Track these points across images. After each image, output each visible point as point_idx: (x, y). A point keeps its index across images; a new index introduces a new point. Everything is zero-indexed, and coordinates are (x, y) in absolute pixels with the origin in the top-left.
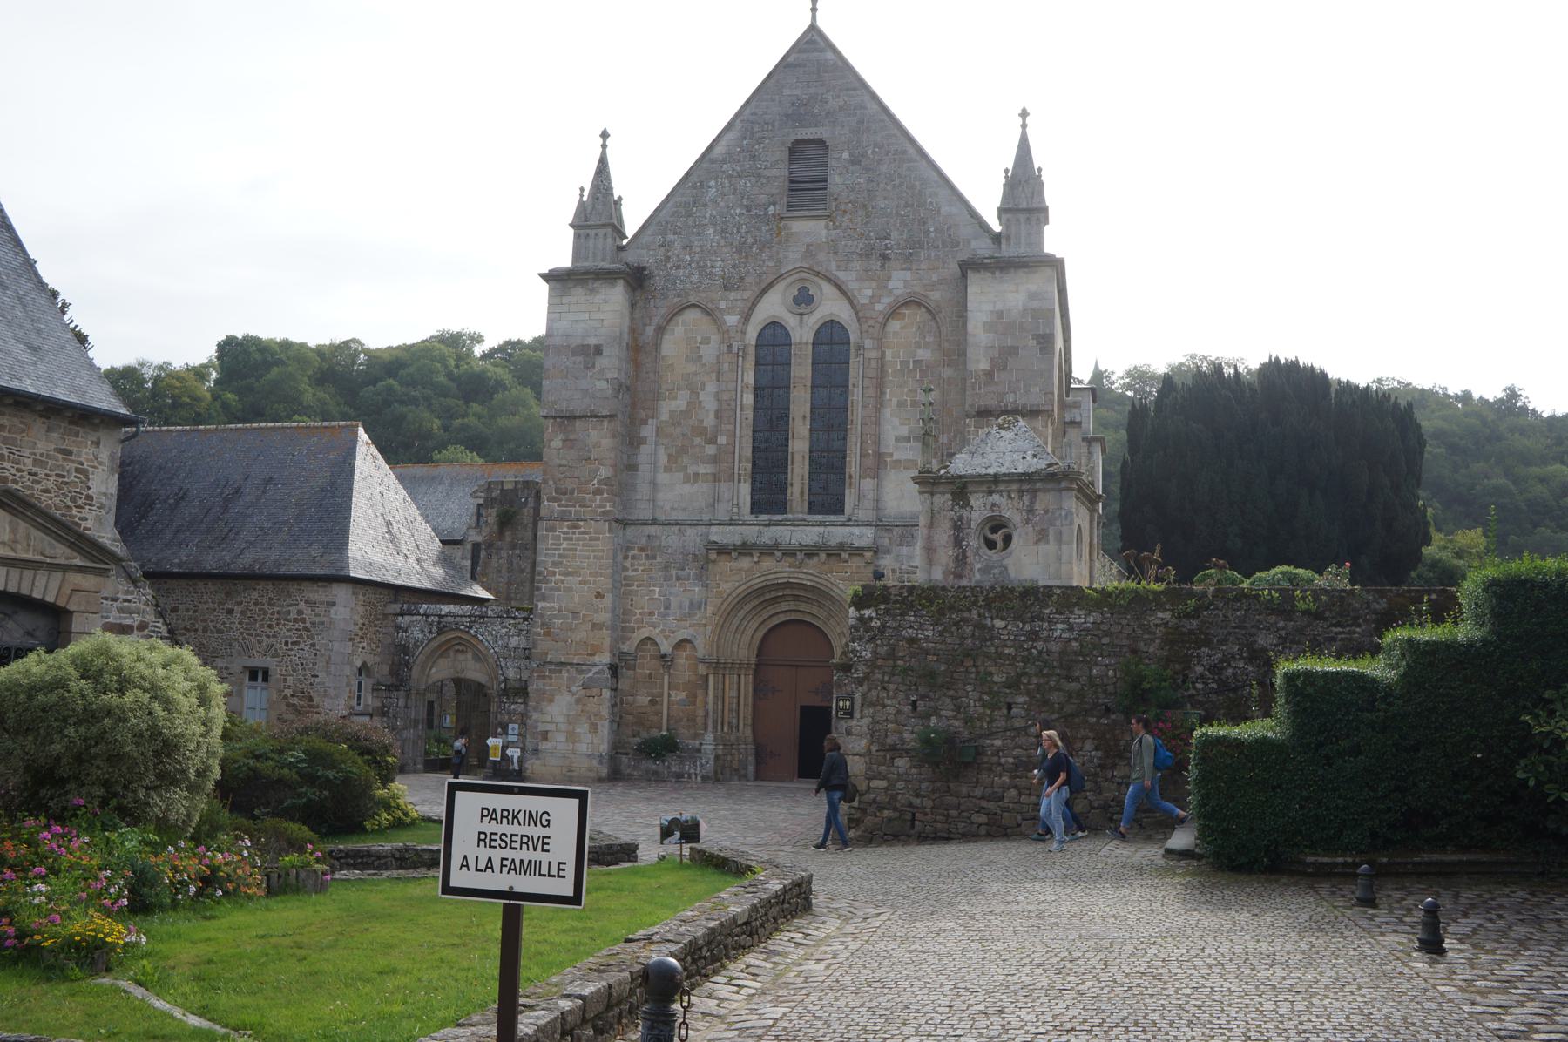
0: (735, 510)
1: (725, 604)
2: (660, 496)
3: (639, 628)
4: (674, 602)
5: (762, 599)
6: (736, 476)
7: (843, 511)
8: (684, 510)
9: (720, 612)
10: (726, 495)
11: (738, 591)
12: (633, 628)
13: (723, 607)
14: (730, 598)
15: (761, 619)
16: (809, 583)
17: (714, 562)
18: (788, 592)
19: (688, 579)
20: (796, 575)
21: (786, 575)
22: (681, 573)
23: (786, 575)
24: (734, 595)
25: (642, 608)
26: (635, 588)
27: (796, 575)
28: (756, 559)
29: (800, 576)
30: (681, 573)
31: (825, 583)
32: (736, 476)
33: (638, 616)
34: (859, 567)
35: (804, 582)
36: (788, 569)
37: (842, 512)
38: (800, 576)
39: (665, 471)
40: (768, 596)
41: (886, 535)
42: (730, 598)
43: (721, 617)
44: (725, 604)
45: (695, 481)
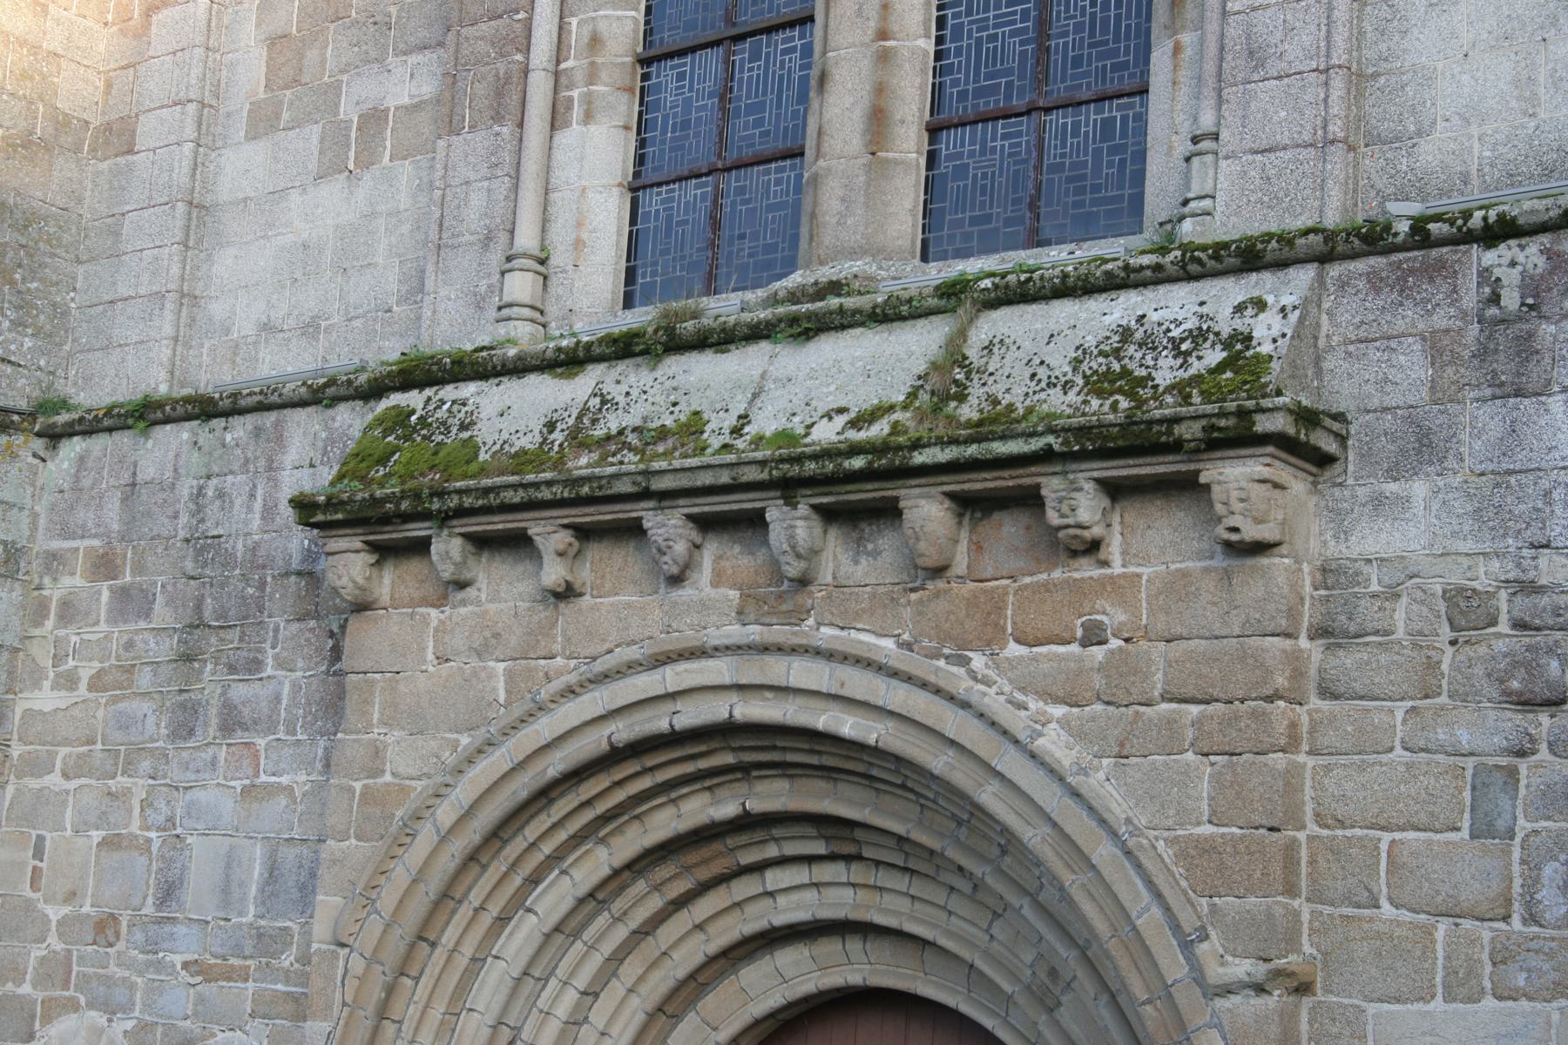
0: (521, 286)
1: (401, 875)
2: (225, 265)
3: (53, 1009)
4: (202, 856)
5: (632, 840)
6: (539, 88)
7: (1137, 203)
8: (310, 329)
9: (375, 926)
10: (477, 200)
11: (464, 792)
12: (26, 1004)
13: (388, 899)
14: (426, 837)
15: (660, 983)
16: (848, 725)
17: (362, 607)
18: (770, 796)
19: (272, 729)
20: (778, 670)
21: (718, 670)
22: (239, 692)
23: (718, 670)
24: (446, 814)
25: (71, 897)
26: (54, 780)
27: (778, 670)
28: (553, 573)
29: (802, 672)
30: (239, 692)
31: (952, 722)
32: (539, 88)
33: (55, 942)
34: (1176, 587)
35: (825, 719)
36: (734, 632)
37: (1130, 212)
38: (802, 672)
39: (252, 136)
40: (664, 823)
41: (1408, 317)
42: (426, 837)
43: (373, 960)
44: (401, 875)
45: (367, 160)
